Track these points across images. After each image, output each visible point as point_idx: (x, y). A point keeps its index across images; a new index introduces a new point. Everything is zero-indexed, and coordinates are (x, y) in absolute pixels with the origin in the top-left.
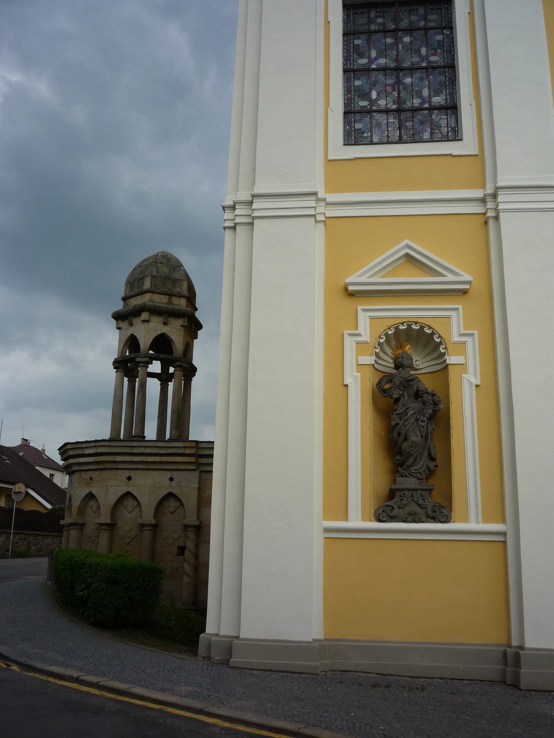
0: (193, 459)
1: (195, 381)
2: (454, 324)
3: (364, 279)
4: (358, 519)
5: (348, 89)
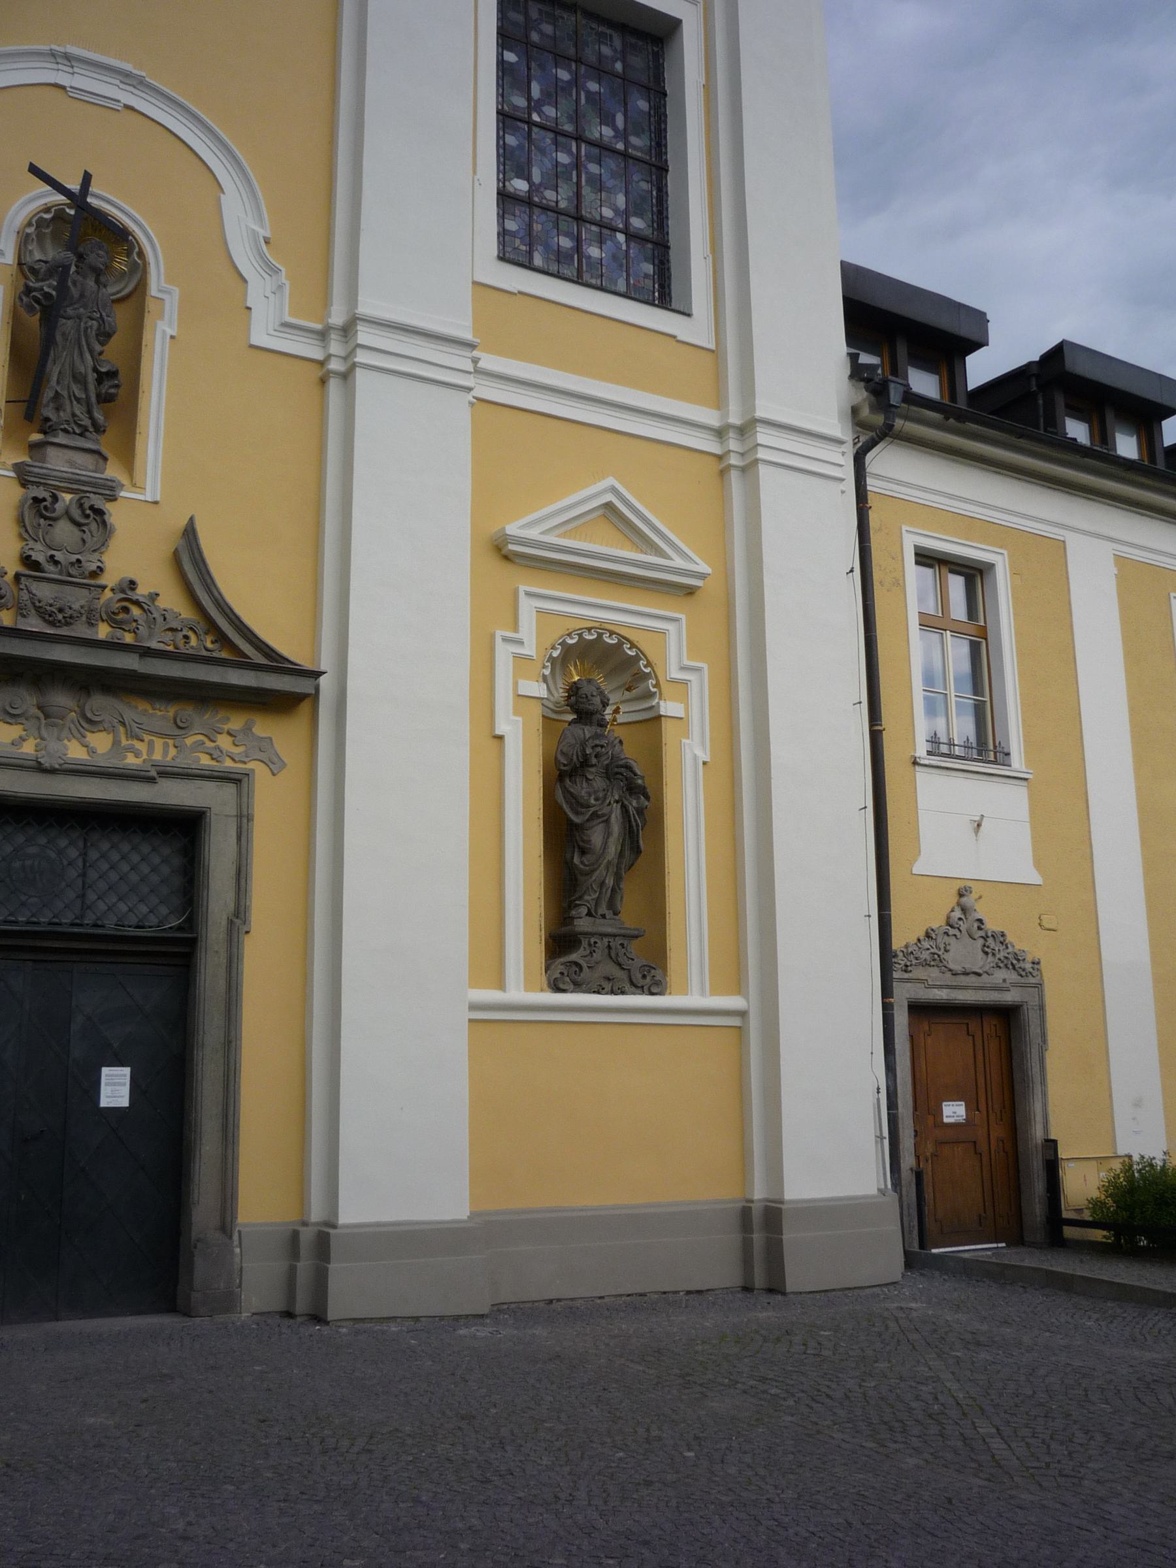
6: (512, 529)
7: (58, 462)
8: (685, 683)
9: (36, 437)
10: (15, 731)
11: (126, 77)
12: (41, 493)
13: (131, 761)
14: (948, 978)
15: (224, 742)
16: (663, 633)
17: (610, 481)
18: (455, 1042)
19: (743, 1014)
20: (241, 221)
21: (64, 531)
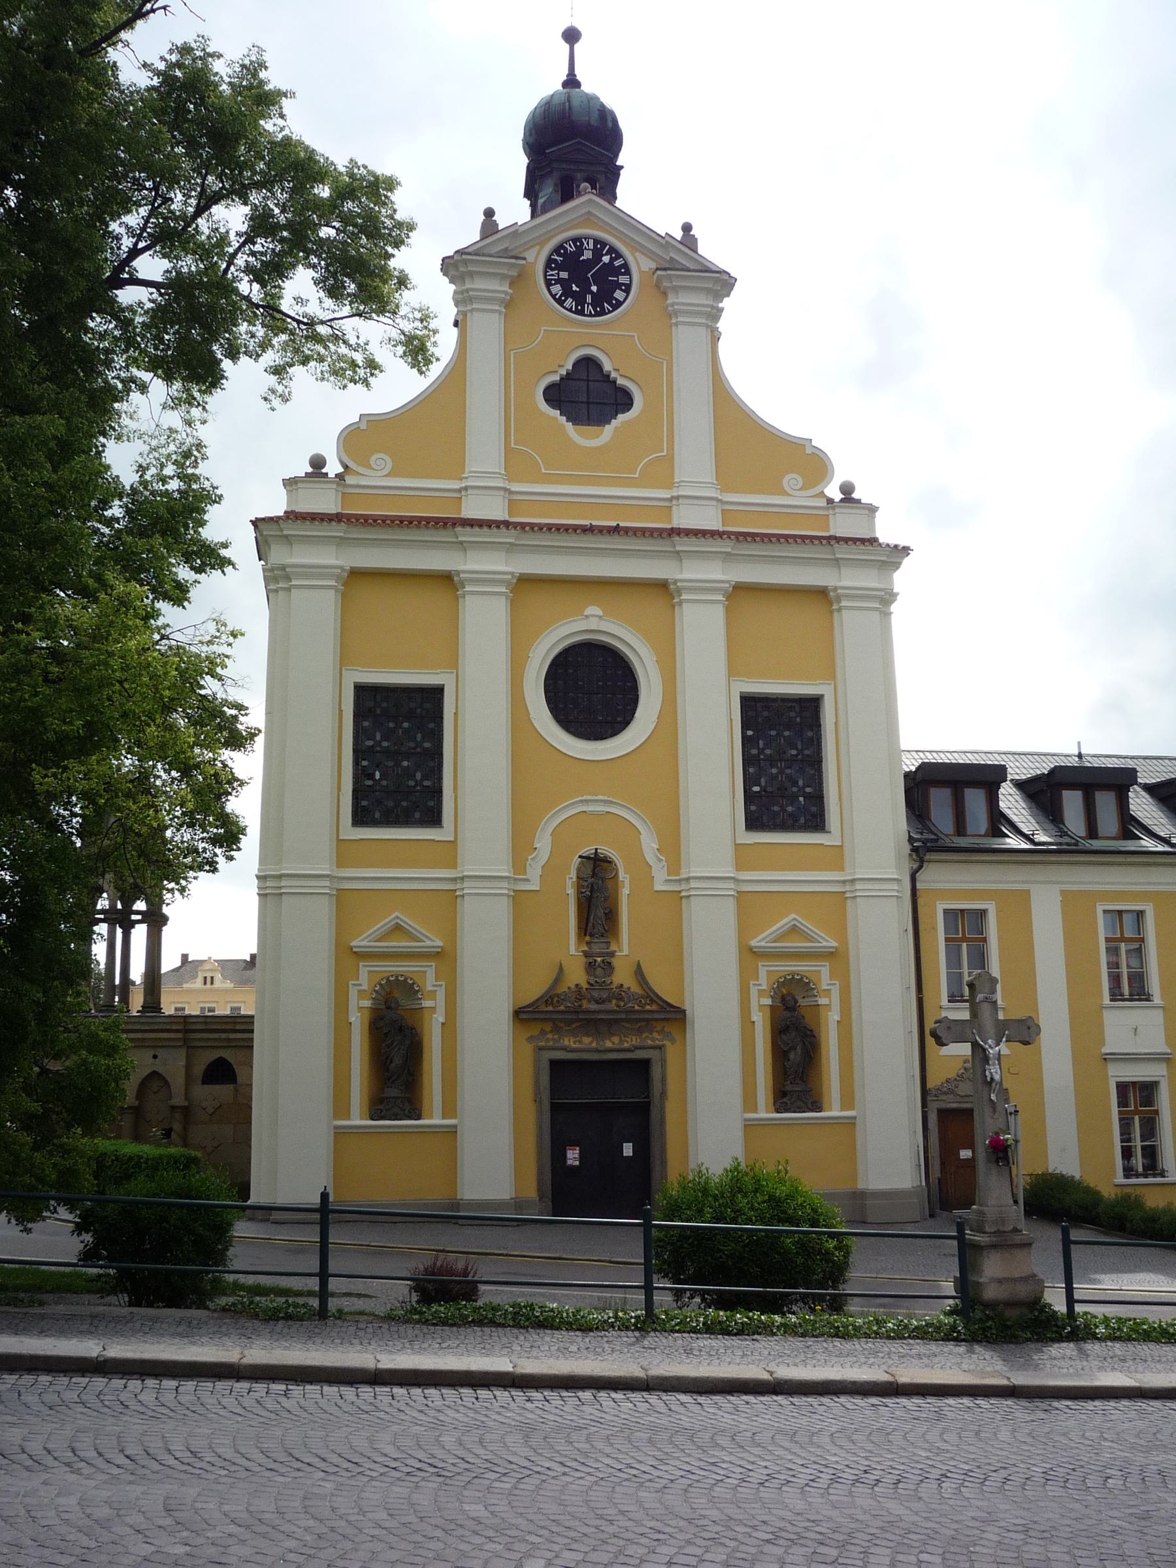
0: (180, 1035)
1: (166, 931)
2: (429, 978)
3: (364, 943)
4: (358, 1119)
5: (356, 762)
6: (753, 943)
7: (596, 949)
8: (829, 990)
9: (588, 938)
10: (590, 1039)
11: (606, 802)
12: (591, 960)
13: (626, 1045)
14: (958, 1099)
15: (655, 1035)
16: (819, 971)
17: (793, 916)
18: (739, 1133)
19: (855, 1118)
20: (649, 844)
21: (599, 971)
